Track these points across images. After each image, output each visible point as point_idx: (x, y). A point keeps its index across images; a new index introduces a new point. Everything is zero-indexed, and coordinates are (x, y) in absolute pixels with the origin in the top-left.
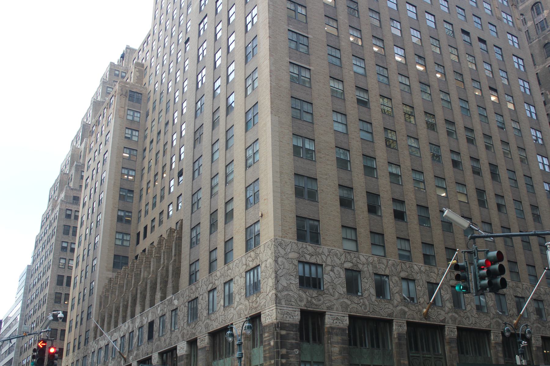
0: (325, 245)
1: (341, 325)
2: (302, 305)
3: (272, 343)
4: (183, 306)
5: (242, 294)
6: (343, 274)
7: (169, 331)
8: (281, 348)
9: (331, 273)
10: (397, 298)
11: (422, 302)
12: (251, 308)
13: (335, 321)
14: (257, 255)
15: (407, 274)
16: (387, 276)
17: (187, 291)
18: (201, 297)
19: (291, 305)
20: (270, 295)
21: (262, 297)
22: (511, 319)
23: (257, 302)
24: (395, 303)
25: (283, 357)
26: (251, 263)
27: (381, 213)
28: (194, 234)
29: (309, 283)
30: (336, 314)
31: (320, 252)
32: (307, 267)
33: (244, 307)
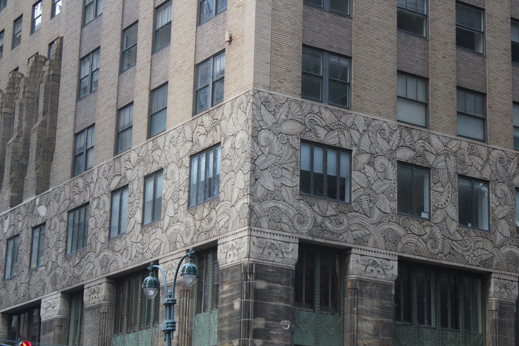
0: (360, 110)
1: (381, 278)
2: (305, 231)
3: (237, 305)
4: (56, 220)
5: (182, 202)
6: (392, 172)
7: (26, 270)
8: (255, 316)
10: (504, 229)
12: (198, 232)
13: (369, 268)
14: (216, 123)
16: (486, 182)
17: (67, 188)
18: (95, 203)
19: (281, 230)
20: (238, 206)
21: (221, 210)
23: (210, 220)
24: (499, 238)
25: (257, 334)
26: (202, 139)
27: (484, 49)
28: (86, 70)
29: (322, 186)
30: (373, 254)
31: (349, 123)
32: (318, 153)
33: (182, 229)
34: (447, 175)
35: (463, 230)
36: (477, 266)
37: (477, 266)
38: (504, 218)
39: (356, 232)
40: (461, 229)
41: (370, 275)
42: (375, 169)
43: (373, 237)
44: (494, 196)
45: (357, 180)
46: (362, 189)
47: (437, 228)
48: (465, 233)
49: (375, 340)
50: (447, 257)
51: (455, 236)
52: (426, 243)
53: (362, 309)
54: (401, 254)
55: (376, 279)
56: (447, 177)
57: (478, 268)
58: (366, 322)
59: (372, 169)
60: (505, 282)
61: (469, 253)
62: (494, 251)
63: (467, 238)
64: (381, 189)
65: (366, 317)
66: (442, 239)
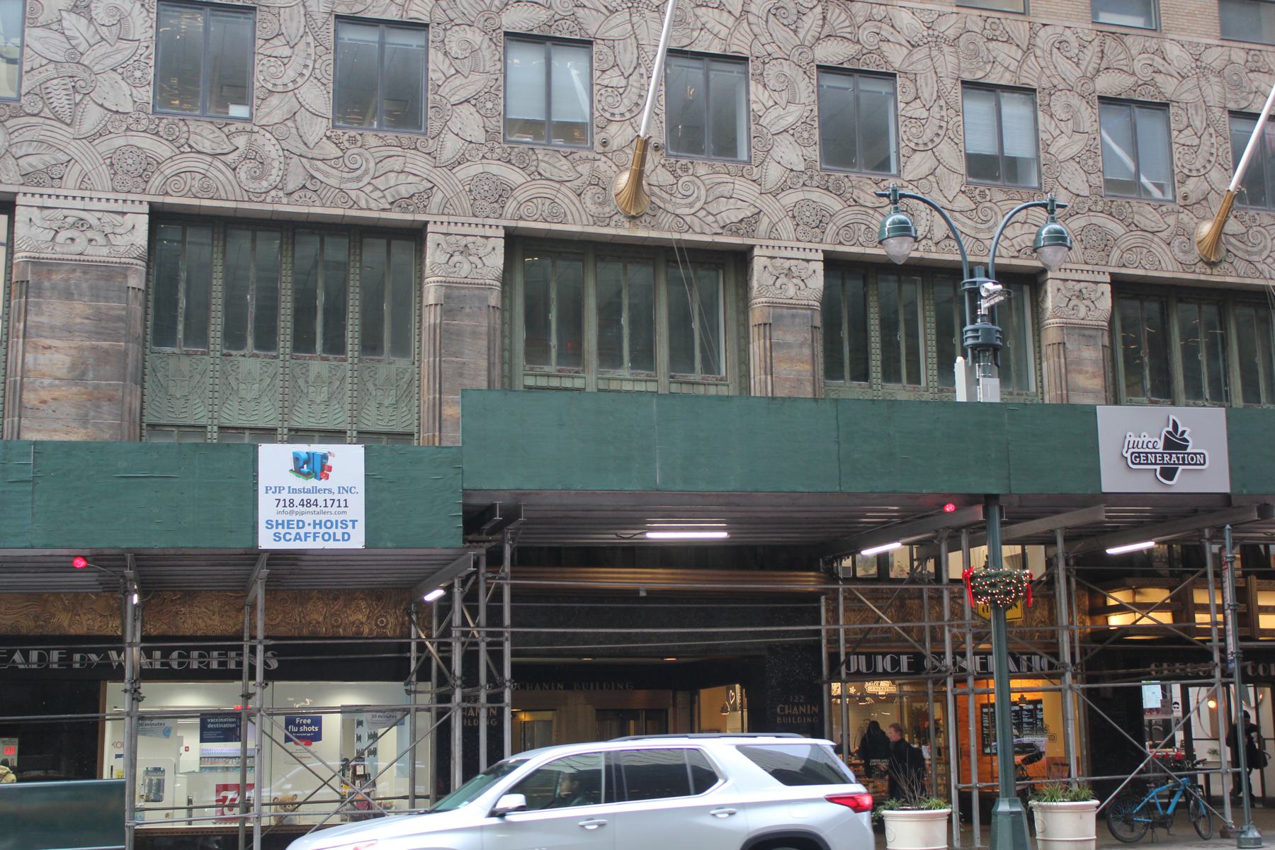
1: (99, 253)
9: (75, 24)
10: (469, 123)
11: (615, 144)
15: (543, 15)
16: (422, 27)
22: (1185, 217)
24: (451, 147)
30: (79, 204)
34: (303, 19)
35: (345, 135)
36: (384, 210)
37: (384, 210)
38: (467, 101)
39: (29, 159)
40: (340, 132)
41: (65, 249)
42: (91, 20)
43: (77, 168)
44: (440, 55)
45: (37, 46)
46: (51, 66)
47: (268, 136)
48: (353, 140)
49: (75, 389)
50: (296, 196)
51: (322, 148)
52: (234, 169)
53: (39, 326)
54: (159, 199)
55: (82, 258)
56: (303, 23)
57: (384, 215)
58: (48, 352)
59: (84, 21)
60: (463, 241)
61: (361, 185)
62: (438, 176)
63: (356, 151)
64: (110, 62)
65: (48, 342)
66: (282, 159)
